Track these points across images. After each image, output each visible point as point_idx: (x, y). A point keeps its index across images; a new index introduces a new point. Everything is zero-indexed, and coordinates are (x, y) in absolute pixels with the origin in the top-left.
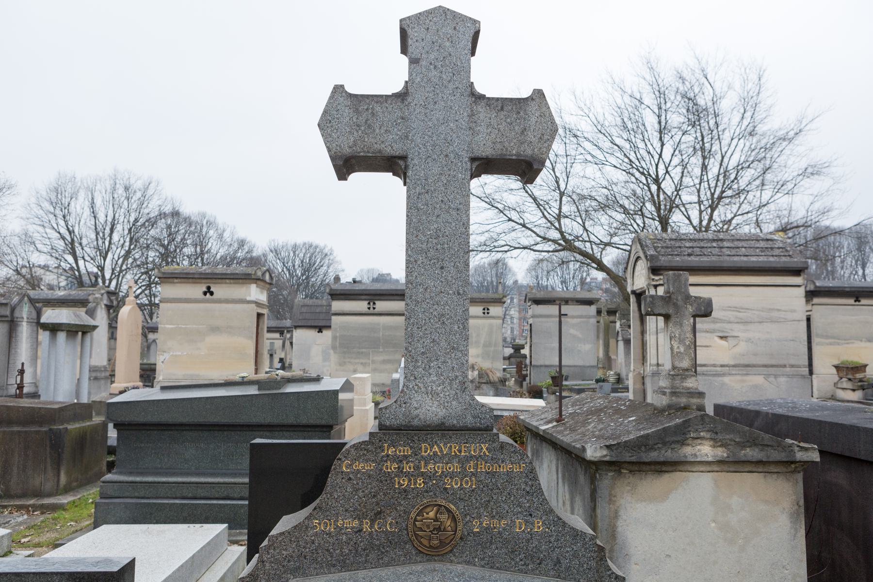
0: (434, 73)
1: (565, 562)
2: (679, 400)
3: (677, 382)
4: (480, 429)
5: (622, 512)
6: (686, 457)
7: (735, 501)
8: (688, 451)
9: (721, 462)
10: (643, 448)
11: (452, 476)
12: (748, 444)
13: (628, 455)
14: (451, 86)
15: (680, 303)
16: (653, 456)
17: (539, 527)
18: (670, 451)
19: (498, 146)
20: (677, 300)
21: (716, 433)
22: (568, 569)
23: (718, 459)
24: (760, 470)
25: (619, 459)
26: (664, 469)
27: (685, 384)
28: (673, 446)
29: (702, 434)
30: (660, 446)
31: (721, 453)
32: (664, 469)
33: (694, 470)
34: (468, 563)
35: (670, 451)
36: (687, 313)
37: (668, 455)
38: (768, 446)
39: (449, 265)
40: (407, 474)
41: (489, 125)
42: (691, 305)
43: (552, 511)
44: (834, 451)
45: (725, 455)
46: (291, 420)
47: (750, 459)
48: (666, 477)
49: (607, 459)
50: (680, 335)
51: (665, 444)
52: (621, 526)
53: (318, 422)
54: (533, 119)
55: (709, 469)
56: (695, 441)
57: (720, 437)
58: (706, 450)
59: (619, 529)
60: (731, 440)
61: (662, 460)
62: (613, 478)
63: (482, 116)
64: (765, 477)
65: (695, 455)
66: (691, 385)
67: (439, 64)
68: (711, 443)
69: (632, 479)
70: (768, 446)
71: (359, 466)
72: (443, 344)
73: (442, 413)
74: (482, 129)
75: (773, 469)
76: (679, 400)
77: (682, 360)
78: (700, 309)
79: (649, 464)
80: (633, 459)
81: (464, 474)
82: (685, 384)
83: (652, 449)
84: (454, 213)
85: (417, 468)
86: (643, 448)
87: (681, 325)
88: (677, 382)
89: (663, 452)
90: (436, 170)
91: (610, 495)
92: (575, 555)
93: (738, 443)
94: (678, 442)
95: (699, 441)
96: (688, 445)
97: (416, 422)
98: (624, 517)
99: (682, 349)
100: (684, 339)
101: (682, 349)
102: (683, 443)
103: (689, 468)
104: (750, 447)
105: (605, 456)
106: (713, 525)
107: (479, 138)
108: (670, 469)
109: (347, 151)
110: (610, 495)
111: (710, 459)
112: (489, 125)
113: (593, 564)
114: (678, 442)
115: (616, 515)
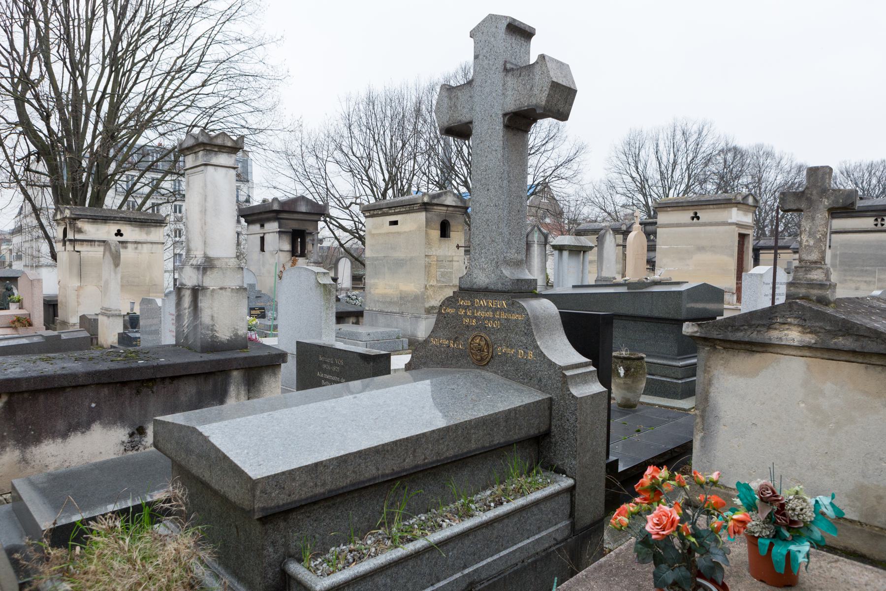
0: (486, 61)
1: (544, 381)
2: (798, 290)
3: (801, 274)
4: (504, 292)
5: (715, 381)
6: (770, 339)
7: (828, 387)
8: (774, 335)
9: (809, 347)
10: (730, 328)
11: (489, 319)
12: (841, 333)
13: (715, 333)
14: (494, 68)
15: (815, 197)
16: (739, 336)
17: (531, 355)
18: (755, 333)
19: (518, 102)
20: (811, 194)
21: (805, 320)
22: (545, 385)
23: (804, 344)
24: (860, 361)
25: (708, 336)
26: (754, 349)
27: (809, 276)
28: (758, 329)
29: (789, 320)
30: (746, 327)
31: (810, 339)
32: (735, 347)
33: (785, 353)
34: (495, 373)
35: (755, 333)
36: (821, 207)
37: (754, 336)
38: (865, 337)
39: (491, 187)
40: (469, 317)
41: (513, 89)
42: (828, 198)
43: (538, 347)
44: (656, 314)
45: (813, 341)
46: (647, 313)
47: (840, 347)
48: (758, 356)
49: (698, 334)
50: (810, 228)
51: (750, 326)
52: (714, 392)
53: (667, 316)
54: (537, 78)
55: (800, 353)
56: (783, 326)
57: (808, 324)
58: (794, 335)
59: (712, 395)
60: (821, 328)
61: (747, 340)
62: (709, 352)
63: (509, 83)
64: (866, 368)
65: (781, 339)
66: (816, 277)
67: (488, 55)
68: (800, 329)
69: (726, 355)
70: (865, 337)
71: (448, 310)
72: (488, 238)
73: (487, 281)
74: (509, 93)
75: (874, 360)
76: (798, 290)
77: (810, 253)
78: (838, 202)
79: (736, 342)
80: (720, 337)
81: (494, 319)
82: (809, 276)
83: (738, 330)
84: (494, 153)
85: (473, 313)
86: (730, 328)
87: (813, 219)
88: (801, 274)
89: (749, 333)
90: (486, 127)
91: (705, 365)
92: (550, 378)
93: (829, 331)
94: (764, 325)
95: (787, 326)
96: (776, 329)
97: (475, 287)
98: (717, 386)
99: (812, 243)
100: (815, 233)
101: (812, 243)
102: (769, 327)
103: (779, 351)
104: (842, 336)
105: (697, 332)
106: (803, 405)
107: (508, 99)
108: (760, 349)
109: (446, 124)
110: (705, 365)
111: (796, 344)
112: (513, 89)
113: (560, 385)
114: (764, 325)
115: (710, 383)
